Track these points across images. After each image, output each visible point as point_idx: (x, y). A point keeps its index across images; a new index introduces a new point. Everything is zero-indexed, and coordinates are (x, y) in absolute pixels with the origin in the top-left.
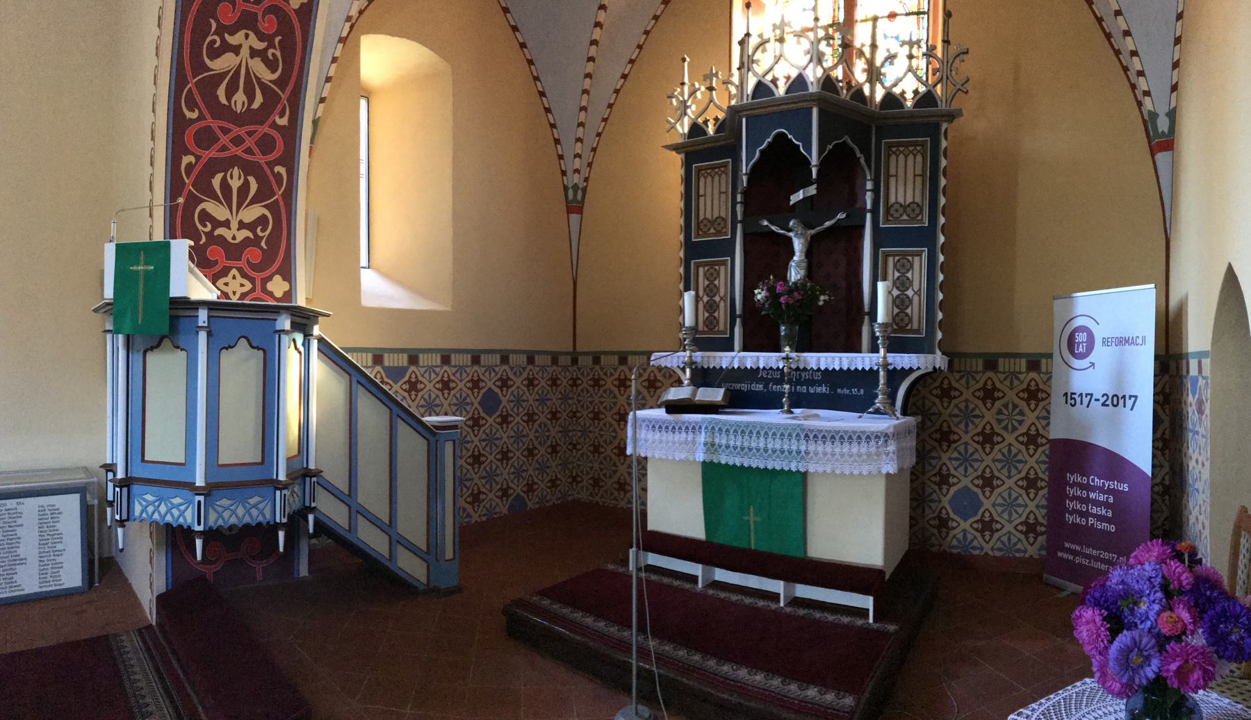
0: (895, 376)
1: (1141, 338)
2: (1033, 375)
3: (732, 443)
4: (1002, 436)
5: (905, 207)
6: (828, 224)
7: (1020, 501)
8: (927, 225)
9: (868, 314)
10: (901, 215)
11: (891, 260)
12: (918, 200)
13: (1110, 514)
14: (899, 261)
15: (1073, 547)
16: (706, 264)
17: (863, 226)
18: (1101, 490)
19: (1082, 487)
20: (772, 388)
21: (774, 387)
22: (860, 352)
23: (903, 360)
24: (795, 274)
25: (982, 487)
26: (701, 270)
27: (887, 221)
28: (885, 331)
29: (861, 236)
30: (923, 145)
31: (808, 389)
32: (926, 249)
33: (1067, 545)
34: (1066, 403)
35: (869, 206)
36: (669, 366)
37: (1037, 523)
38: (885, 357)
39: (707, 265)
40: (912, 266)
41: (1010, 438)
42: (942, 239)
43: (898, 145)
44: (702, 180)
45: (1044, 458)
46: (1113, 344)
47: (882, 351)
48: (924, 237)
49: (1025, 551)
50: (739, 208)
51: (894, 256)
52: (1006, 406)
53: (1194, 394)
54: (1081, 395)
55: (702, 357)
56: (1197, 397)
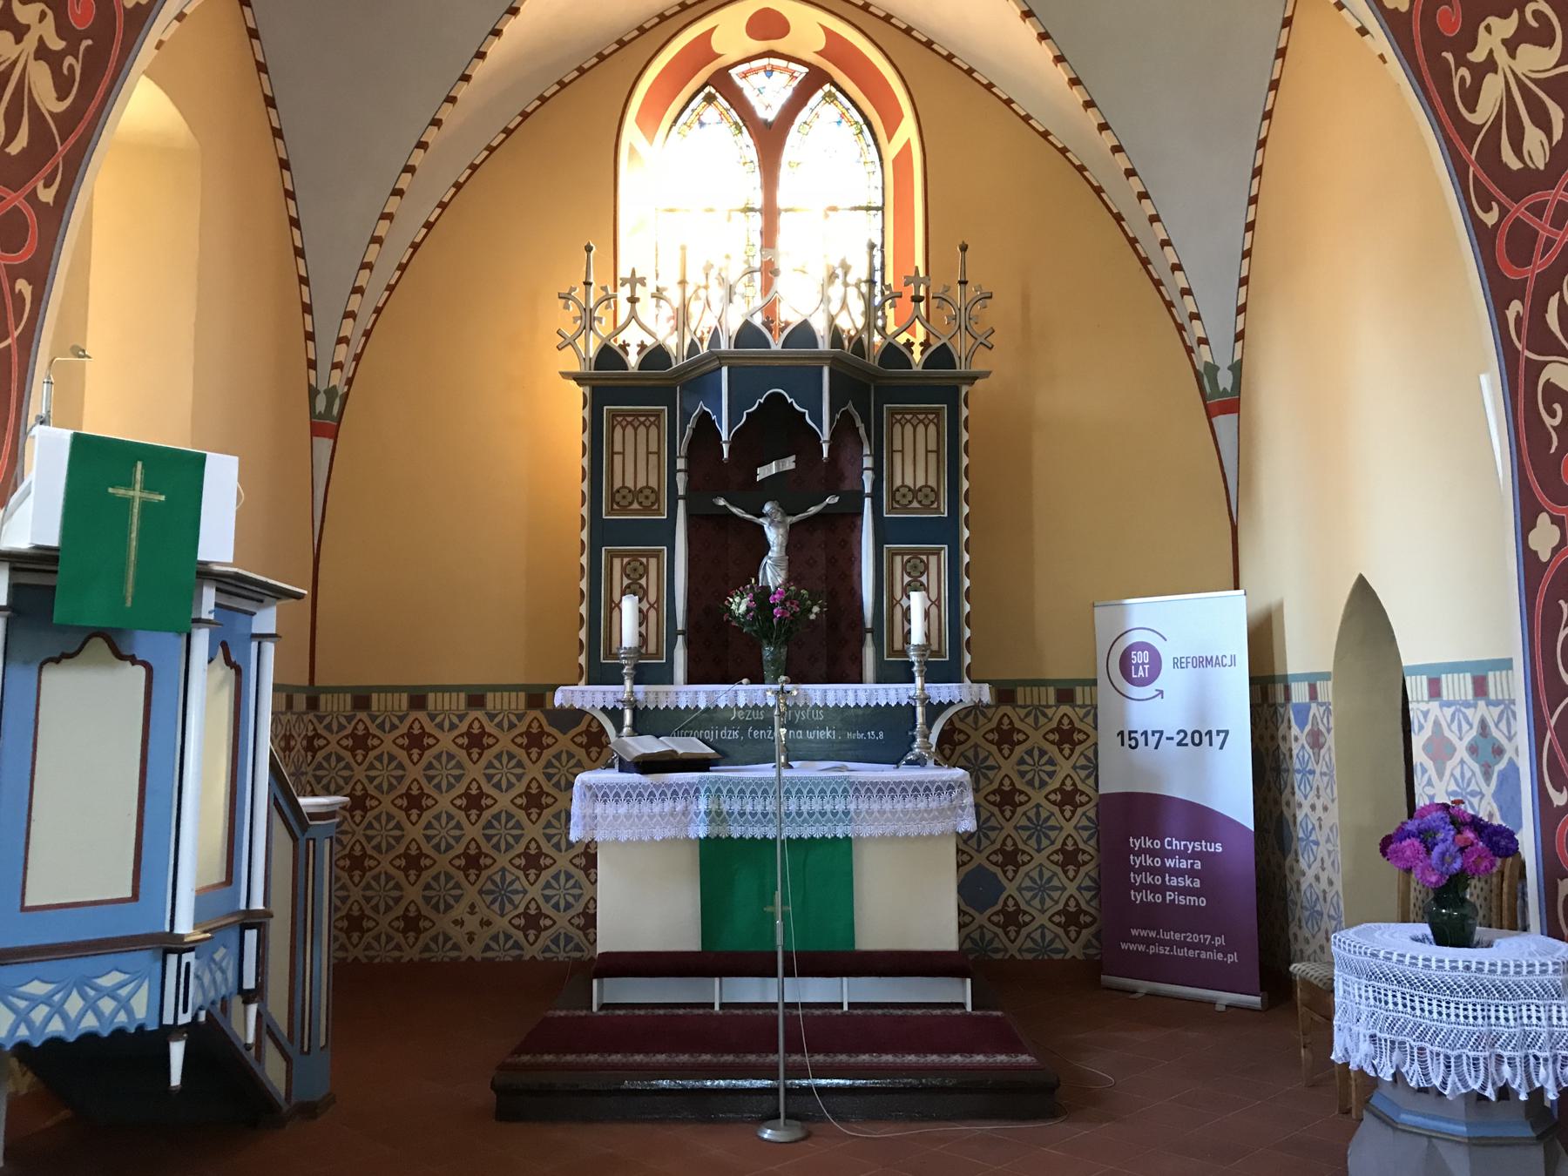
0: (934, 711)
1: (1229, 658)
2: (1065, 709)
3: (749, 808)
4: (1027, 795)
5: (915, 492)
6: (813, 510)
7: (1055, 882)
8: (946, 515)
9: (871, 631)
10: (910, 502)
11: (898, 559)
12: (932, 482)
13: (1197, 884)
14: (909, 561)
15: (1144, 933)
16: (621, 555)
17: (861, 514)
18: (1183, 854)
19: (1153, 853)
20: (752, 734)
21: (756, 733)
22: (859, 680)
23: (942, 692)
24: (772, 574)
25: (1002, 866)
26: (617, 563)
27: (892, 509)
28: (923, 655)
29: (856, 528)
30: (937, 413)
31: (804, 735)
32: (946, 546)
33: (1134, 932)
34: (1123, 745)
35: (868, 489)
36: (587, 707)
37: (1080, 911)
38: (923, 689)
39: (626, 556)
40: (927, 567)
41: (1038, 797)
42: (966, 533)
43: (903, 412)
44: (618, 431)
45: (1085, 822)
46: (1190, 665)
47: (918, 680)
48: (945, 531)
49: (1066, 951)
50: (681, 479)
51: (903, 555)
52: (1030, 753)
53: (1302, 726)
54: (1145, 733)
55: (646, 693)
56: (1308, 728)
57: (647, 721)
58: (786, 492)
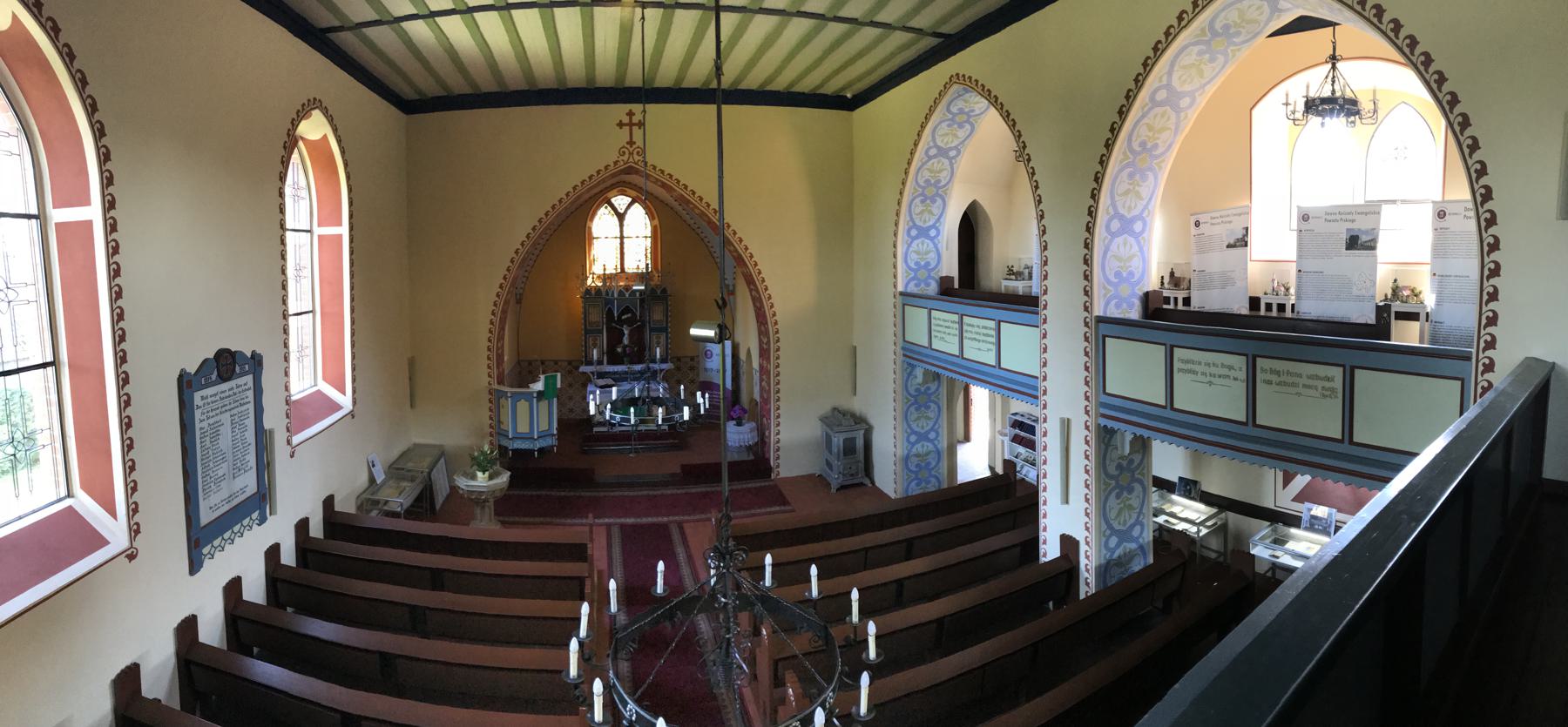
0: (661, 370)
23: (664, 366)
24: (626, 341)
48: (665, 330)
50: (605, 320)
57: (601, 375)
58: (629, 322)
